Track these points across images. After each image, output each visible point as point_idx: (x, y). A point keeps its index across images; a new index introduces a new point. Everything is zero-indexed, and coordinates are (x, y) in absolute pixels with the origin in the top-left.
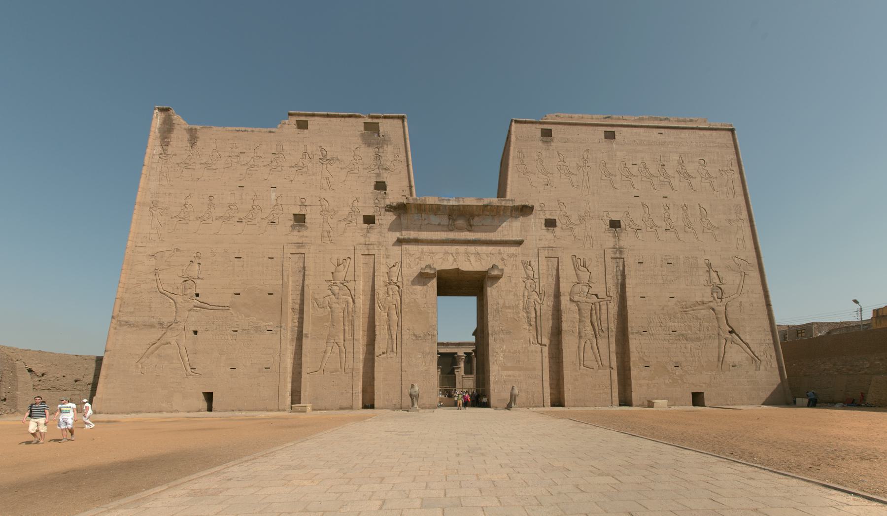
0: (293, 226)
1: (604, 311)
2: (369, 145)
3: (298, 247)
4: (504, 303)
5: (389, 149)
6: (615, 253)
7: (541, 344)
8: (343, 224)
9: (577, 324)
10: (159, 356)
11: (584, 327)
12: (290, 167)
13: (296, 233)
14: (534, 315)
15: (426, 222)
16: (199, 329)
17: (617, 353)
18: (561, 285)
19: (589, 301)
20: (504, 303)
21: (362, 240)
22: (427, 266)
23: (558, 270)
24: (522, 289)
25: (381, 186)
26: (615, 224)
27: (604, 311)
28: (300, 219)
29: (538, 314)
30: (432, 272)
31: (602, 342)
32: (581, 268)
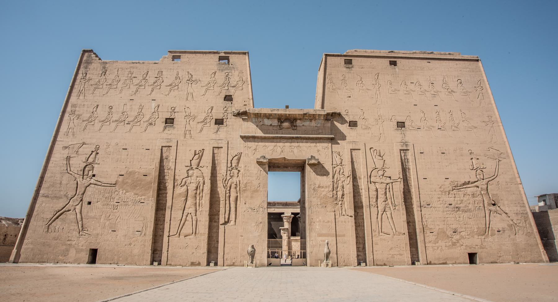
0: (165, 128)
2: (222, 70)
3: (168, 142)
5: (237, 73)
8: (200, 125)
10: (64, 220)
12: (166, 86)
13: (166, 131)
15: (261, 123)
16: (93, 201)
19: (383, 181)
21: (214, 136)
22: (261, 157)
25: (228, 98)
26: (401, 125)
28: (169, 121)
30: (265, 161)
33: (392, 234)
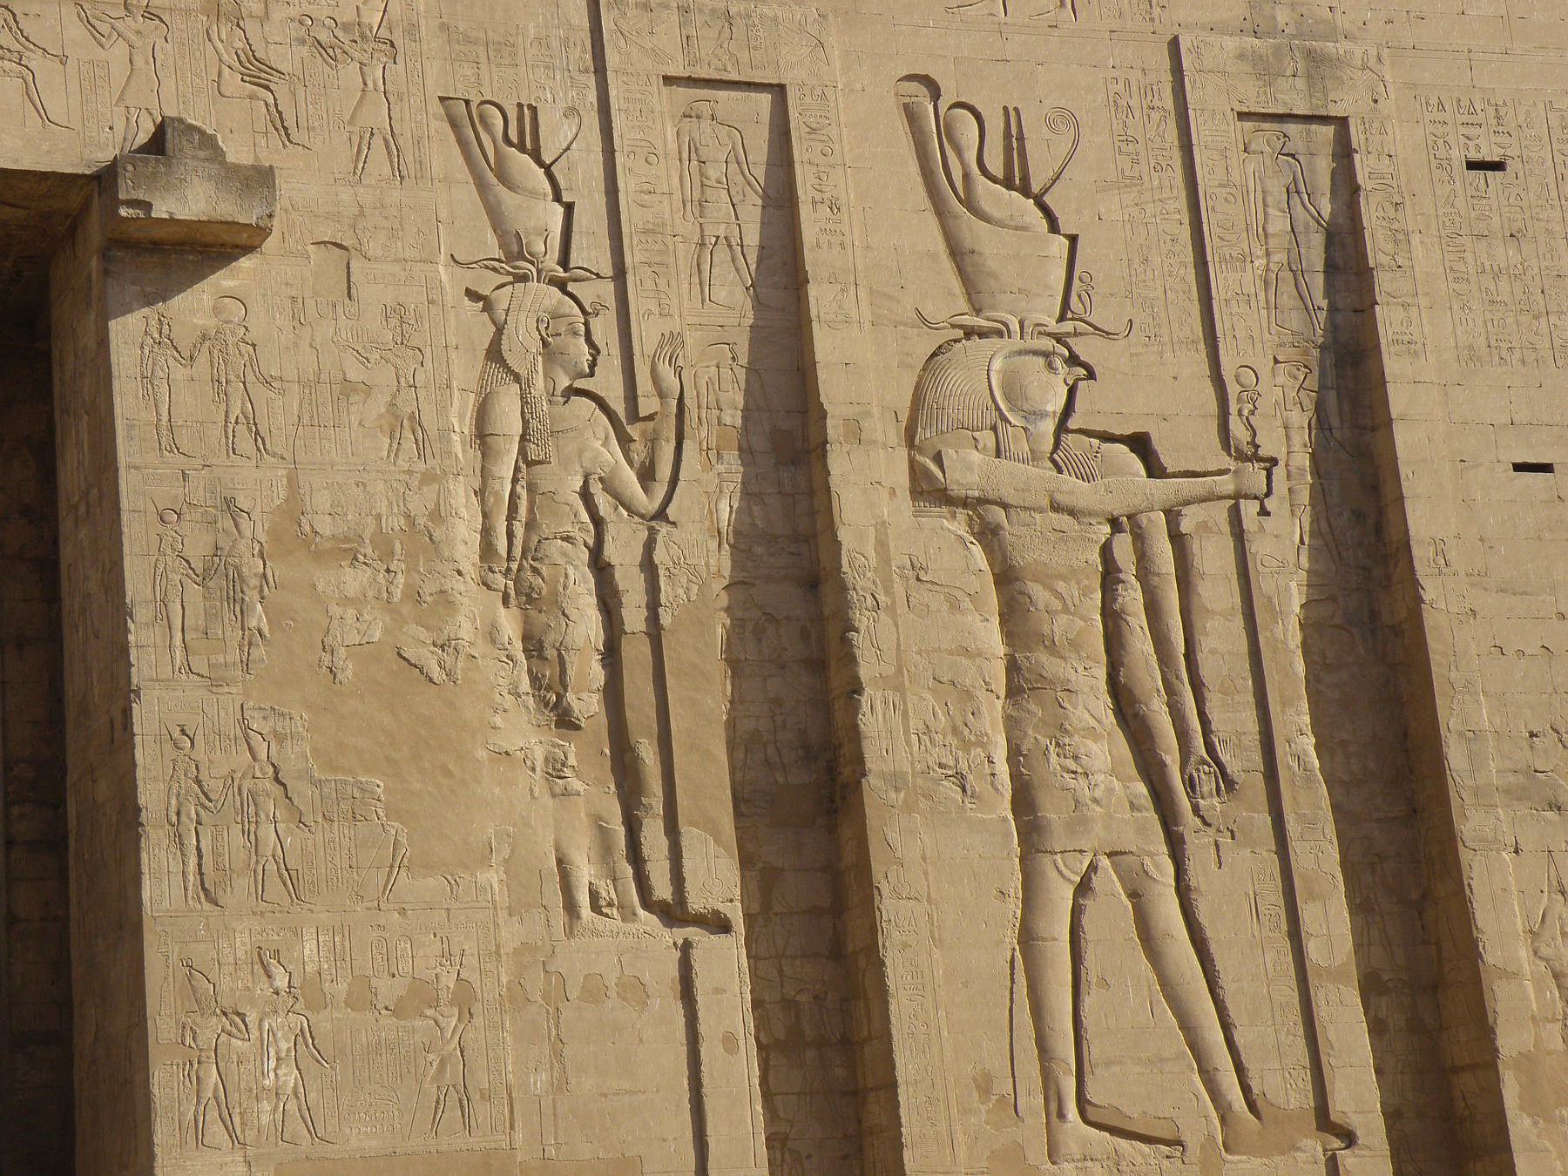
1: (1217, 589)
4: (293, 509)
6: (1265, 71)
7: (674, 913)
9: (993, 709)
11: (1061, 729)
14: (587, 626)
17: (1370, 987)
18: (826, 346)
19: (1073, 489)
20: (293, 509)
23: (781, 201)
24: (466, 369)
27: (1217, 589)
29: (634, 616)
31: (1234, 879)
32: (990, 194)
33: (1198, 1121)
